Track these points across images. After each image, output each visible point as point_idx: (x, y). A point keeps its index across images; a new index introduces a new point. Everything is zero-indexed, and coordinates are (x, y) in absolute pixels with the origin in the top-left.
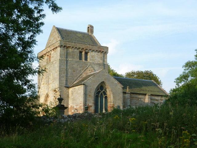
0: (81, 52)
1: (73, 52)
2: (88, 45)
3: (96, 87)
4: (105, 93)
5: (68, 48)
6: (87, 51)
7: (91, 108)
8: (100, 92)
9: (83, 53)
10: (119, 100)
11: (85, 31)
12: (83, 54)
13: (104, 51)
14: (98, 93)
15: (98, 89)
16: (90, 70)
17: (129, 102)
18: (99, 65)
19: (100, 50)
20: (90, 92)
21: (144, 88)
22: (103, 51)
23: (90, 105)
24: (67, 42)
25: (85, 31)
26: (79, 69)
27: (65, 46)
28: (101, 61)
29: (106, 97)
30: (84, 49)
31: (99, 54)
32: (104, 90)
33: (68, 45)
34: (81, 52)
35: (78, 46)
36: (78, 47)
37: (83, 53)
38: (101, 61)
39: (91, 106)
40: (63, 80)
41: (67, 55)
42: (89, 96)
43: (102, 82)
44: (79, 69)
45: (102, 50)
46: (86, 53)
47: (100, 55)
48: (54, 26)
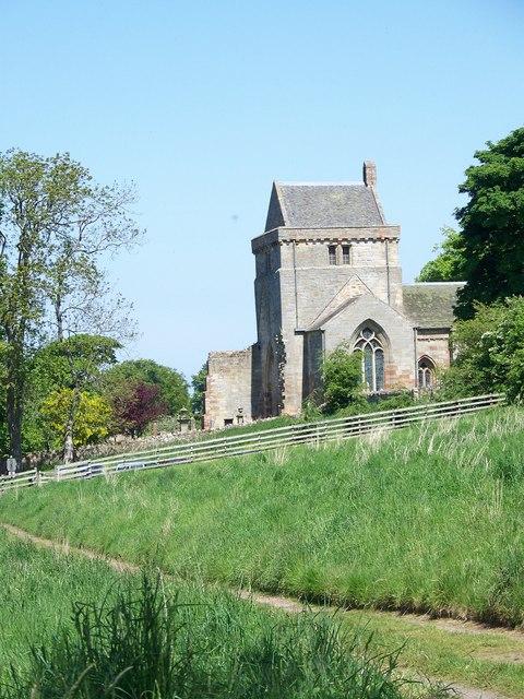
9: (339, 250)
10: (407, 355)
18: (378, 270)
27: (292, 241)
33: (298, 238)
34: (332, 250)
35: (323, 234)
37: (339, 250)
46: (346, 250)
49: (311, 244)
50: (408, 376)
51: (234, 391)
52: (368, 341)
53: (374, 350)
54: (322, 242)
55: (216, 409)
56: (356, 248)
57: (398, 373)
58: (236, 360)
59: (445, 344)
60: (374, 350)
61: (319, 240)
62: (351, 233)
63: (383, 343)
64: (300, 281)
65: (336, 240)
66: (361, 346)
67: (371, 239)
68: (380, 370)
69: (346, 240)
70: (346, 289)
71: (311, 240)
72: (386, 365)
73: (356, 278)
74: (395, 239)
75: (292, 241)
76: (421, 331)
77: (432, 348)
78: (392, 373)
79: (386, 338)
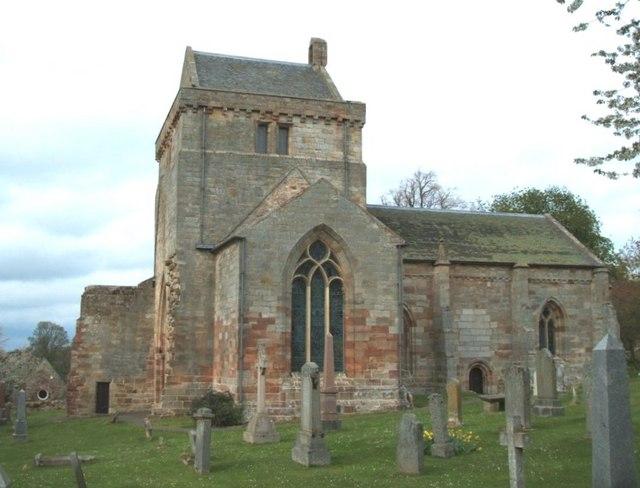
0: (263, 126)
1: (231, 125)
2: (288, 100)
3: (289, 248)
4: (331, 269)
5: (210, 111)
6: (283, 120)
7: (270, 328)
8: (311, 264)
9: (272, 127)
10: (386, 291)
11: (302, 58)
12: (274, 129)
13: (351, 118)
14: (305, 268)
15: (304, 255)
16: (294, 188)
17: (447, 295)
18: (331, 165)
19: (332, 113)
20: (266, 266)
21: (508, 241)
22: (344, 120)
23: (264, 316)
25: (302, 58)
26: (255, 184)
27: (201, 107)
28: (339, 155)
29: (337, 286)
30: (271, 113)
31: (333, 127)
32: (327, 259)
33: (213, 104)
36: (249, 109)
37: (272, 127)
38: (339, 155)
39: (271, 321)
41: (205, 137)
42: (263, 282)
43: (316, 229)
44: (255, 184)
45: (343, 116)
46: (285, 128)
47: (335, 132)
48: (188, 49)
49: (231, 114)
50: (385, 330)
51: (114, 342)
52: (319, 264)
53: (328, 281)
54: (249, 114)
55: (87, 366)
56: (302, 131)
57: (370, 322)
58: (119, 300)
60: (328, 281)
62: (292, 106)
63: (344, 268)
64: (212, 169)
66: (307, 274)
68: (337, 315)
70: (280, 192)
72: (347, 310)
73: (296, 174)
75: (201, 107)
76: (406, 261)
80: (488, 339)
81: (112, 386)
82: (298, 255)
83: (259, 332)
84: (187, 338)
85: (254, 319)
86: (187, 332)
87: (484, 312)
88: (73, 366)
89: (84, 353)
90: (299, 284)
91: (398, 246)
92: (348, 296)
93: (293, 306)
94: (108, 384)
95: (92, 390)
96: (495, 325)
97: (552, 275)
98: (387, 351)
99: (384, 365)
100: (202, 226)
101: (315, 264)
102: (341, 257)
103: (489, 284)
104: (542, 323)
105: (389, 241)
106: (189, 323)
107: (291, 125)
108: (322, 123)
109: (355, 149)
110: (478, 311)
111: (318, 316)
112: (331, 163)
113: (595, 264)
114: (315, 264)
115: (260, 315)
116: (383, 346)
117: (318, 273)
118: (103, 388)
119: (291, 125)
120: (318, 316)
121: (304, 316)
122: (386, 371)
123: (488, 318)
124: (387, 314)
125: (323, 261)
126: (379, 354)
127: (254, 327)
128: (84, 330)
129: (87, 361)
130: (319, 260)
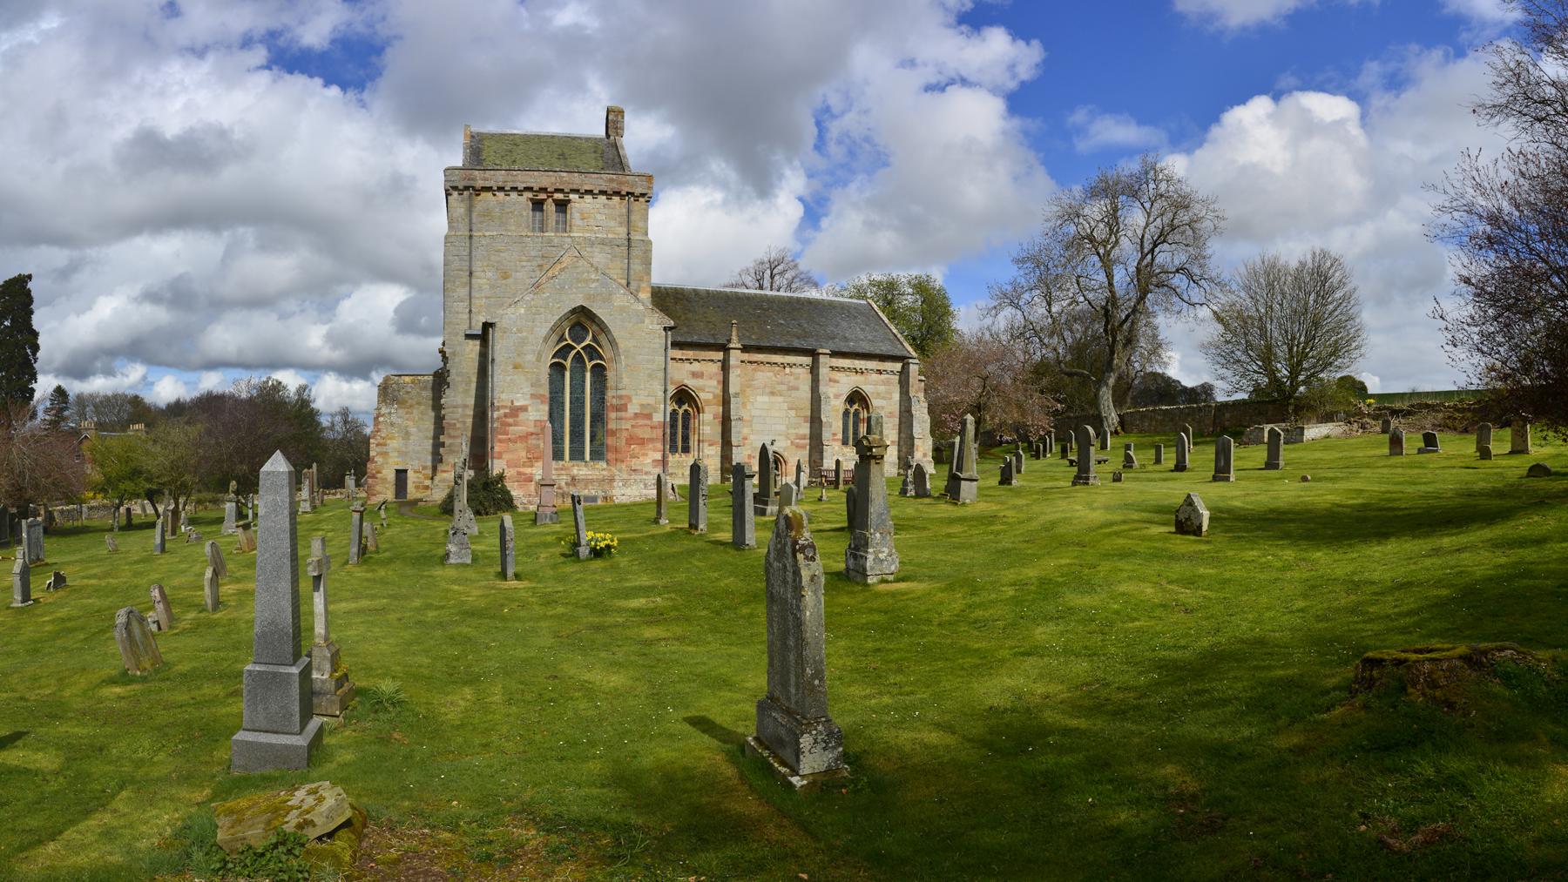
2: (565, 174)
4: (592, 352)
7: (522, 416)
9: (550, 207)
11: (600, 131)
14: (563, 352)
15: (562, 338)
19: (615, 186)
22: (628, 193)
23: (517, 404)
24: (477, 172)
29: (599, 371)
31: (616, 199)
34: (538, 205)
36: (521, 187)
37: (550, 207)
39: (524, 409)
40: (460, 310)
43: (574, 311)
46: (562, 206)
50: (649, 416)
52: (579, 348)
53: (589, 365)
54: (520, 192)
55: (385, 454)
56: (578, 204)
57: (633, 408)
59: (715, 368)
60: (589, 365)
61: (514, 189)
62: (576, 180)
63: (606, 352)
65: (543, 190)
67: (602, 193)
69: (561, 191)
71: (501, 189)
74: (643, 195)
75: (466, 188)
77: (695, 375)
78: (621, 408)
79: (613, 343)
80: (783, 428)
81: (410, 474)
82: (555, 338)
83: (510, 420)
84: (458, 425)
85: (506, 407)
86: (457, 419)
87: (780, 399)
88: (372, 453)
89: (382, 441)
90: (557, 368)
91: (665, 329)
92: (611, 383)
93: (551, 393)
94: (406, 471)
95: (391, 476)
96: (793, 413)
97: (859, 364)
98: (651, 440)
99: (647, 455)
100: (470, 311)
101: (575, 348)
102: (602, 338)
103: (788, 370)
104: (846, 413)
105: (654, 325)
106: (460, 410)
107: (569, 201)
108: (603, 198)
109: (641, 224)
110: (774, 399)
111: (577, 403)
112: (611, 241)
113: (908, 355)
114: (575, 348)
115: (512, 402)
116: (645, 433)
117: (578, 356)
118: (401, 474)
119: (569, 201)
120: (577, 403)
121: (563, 403)
122: (649, 461)
123: (785, 406)
124: (651, 401)
125: (583, 344)
126: (642, 442)
127: (506, 415)
128: (381, 419)
129: (384, 449)
130: (579, 344)
